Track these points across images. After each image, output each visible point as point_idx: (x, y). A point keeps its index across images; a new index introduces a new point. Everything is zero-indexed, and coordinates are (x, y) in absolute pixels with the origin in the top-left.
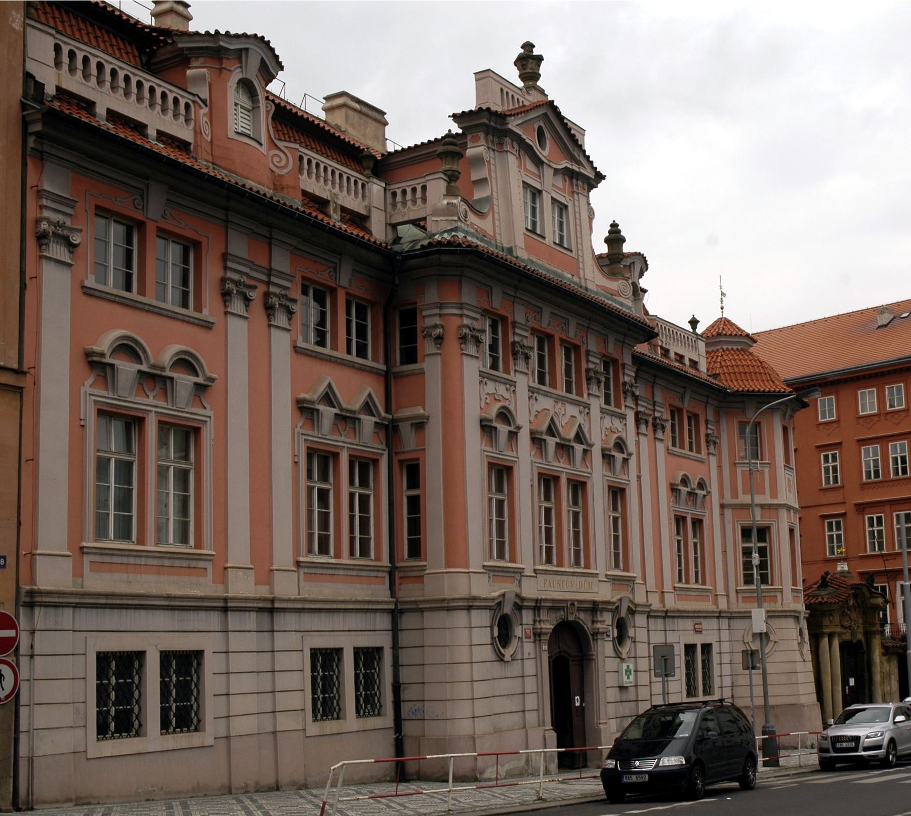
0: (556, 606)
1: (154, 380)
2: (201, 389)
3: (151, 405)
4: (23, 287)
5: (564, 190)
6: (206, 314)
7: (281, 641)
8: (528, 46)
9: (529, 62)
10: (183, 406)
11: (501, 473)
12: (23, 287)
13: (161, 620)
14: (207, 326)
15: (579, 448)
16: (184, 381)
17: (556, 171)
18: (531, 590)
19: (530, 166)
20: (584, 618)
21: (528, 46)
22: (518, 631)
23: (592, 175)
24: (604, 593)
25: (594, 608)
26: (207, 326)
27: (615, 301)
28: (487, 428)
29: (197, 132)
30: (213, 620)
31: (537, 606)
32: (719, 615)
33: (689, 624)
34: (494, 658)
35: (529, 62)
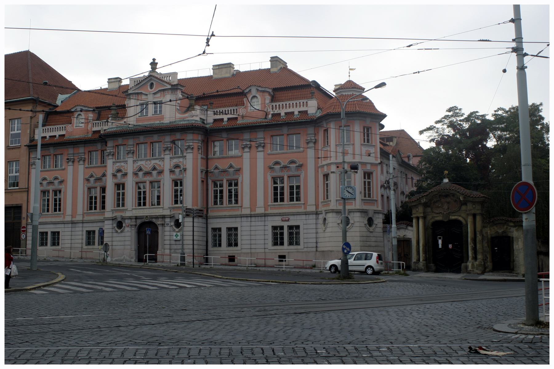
0: (136, 218)
1: (51, 183)
2: (61, 182)
3: (51, 188)
4: (29, 174)
5: (161, 97)
6: (63, 167)
7: (77, 229)
8: (154, 60)
9: (154, 64)
10: (56, 186)
11: (120, 186)
12: (29, 174)
13: (52, 226)
14: (63, 170)
15: (154, 173)
16: (56, 182)
17: (155, 94)
18: (128, 214)
19: (144, 97)
20: (154, 220)
21: (154, 60)
22: (124, 225)
23: (169, 87)
24: (167, 212)
25: (157, 217)
26: (63, 170)
27: (185, 121)
28: (114, 176)
29: (67, 132)
30: (62, 226)
31: (130, 218)
32: (306, 214)
33: (279, 218)
34: (114, 231)
35: (154, 64)
